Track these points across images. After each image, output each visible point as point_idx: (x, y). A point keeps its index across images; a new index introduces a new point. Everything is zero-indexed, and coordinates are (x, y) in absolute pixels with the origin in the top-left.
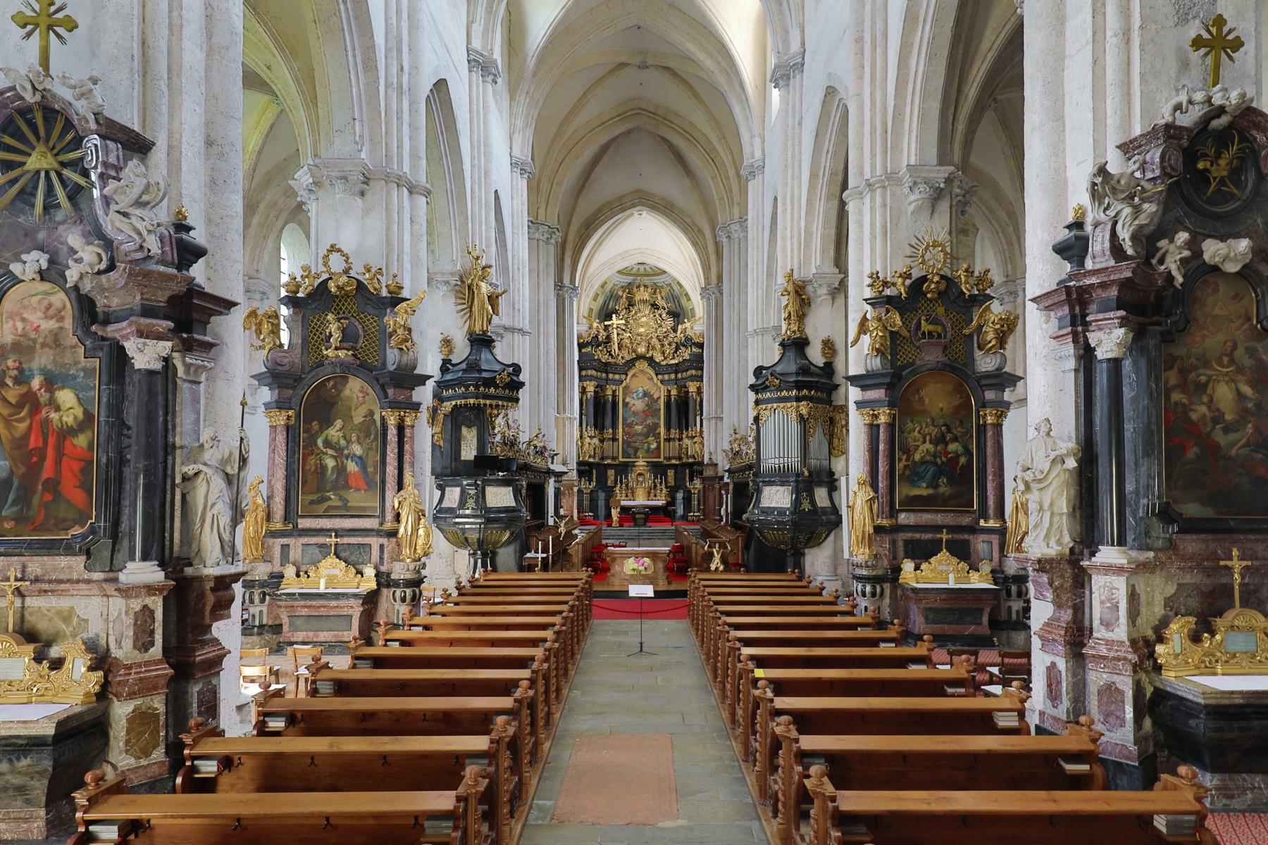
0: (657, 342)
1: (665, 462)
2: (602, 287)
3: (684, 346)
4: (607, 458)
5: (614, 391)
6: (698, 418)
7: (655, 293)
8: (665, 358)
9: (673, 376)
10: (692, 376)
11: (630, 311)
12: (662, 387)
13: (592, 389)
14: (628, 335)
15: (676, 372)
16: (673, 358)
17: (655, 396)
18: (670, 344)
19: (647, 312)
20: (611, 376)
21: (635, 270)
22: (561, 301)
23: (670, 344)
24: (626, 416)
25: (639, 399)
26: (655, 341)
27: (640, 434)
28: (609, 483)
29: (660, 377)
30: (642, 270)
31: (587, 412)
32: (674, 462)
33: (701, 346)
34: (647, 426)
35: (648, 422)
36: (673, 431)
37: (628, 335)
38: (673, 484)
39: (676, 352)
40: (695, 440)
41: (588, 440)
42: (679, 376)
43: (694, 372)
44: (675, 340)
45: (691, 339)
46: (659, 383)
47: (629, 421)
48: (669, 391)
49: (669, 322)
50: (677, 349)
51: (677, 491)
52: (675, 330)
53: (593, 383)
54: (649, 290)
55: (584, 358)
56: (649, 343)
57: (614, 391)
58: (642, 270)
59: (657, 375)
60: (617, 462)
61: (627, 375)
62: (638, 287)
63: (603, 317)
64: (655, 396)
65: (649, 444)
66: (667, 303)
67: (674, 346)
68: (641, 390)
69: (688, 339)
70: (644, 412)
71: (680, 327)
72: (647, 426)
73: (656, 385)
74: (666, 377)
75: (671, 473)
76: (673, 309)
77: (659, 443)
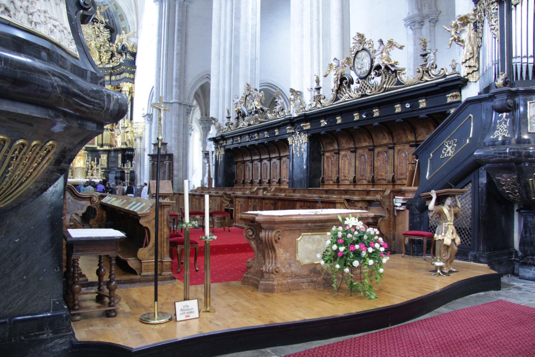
1: (99, 148)
3: (120, 53)
10: (126, 78)
15: (111, 75)
18: (106, 52)
23: (106, 52)
32: (106, 148)
33: (134, 55)
39: (111, 58)
40: (127, 130)
42: (113, 78)
43: (127, 75)
49: (106, 34)
50: (113, 55)
51: (109, 172)
52: (112, 40)
66: (105, 18)
67: (110, 53)
69: (124, 48)
71: (118, 36)
75: (104, 158)
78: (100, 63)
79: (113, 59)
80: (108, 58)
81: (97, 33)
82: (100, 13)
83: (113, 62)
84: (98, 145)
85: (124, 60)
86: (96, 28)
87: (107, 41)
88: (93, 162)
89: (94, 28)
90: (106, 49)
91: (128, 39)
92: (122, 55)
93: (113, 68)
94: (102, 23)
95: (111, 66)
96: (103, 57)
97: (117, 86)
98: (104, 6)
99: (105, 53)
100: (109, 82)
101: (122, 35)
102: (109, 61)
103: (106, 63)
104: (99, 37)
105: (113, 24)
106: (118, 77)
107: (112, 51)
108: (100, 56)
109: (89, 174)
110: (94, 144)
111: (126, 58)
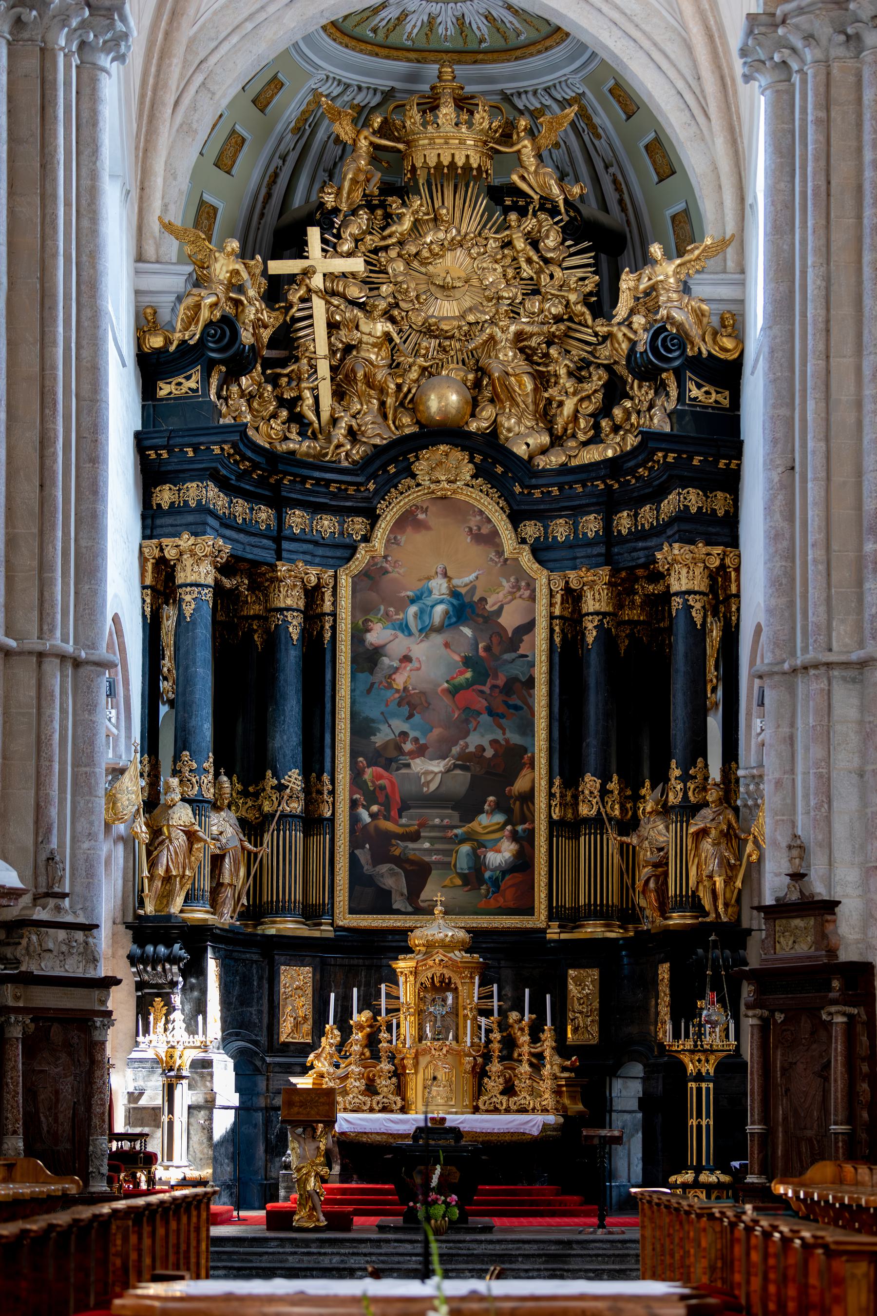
0: (520, 365)
2: (261, 102)
4: (279, 910)
5: (313, 594)
6: (714, 725)
7: (507, 136)
8: (557, 440)
9: (591, 525)
10: (683, 516)
11: (389, 219)
12: (541, 577)
13: (205, 573)
14: (381, 327)
16: (596, 439)
17: (509, 620)
18: (578, 374)
19: (470, 225)
20: (297, 520)
21: (413, 26)
22: (31, 64)
24: (371, 709)
25: (428, 630)
26: (508, 354)
27: (436, 800)
28: (286, 1032)
29: (531, 529)
30: (446, 27)
31: (184, 683)
32: (593, 930)
34: (465, 761)
35: (474, 741)
36: (590, 783)
37: (381, 327)
38: (592, 1036)
39: (605, 411)
41: (182, 815)
42: (624, 522)
43: (693, 499)
44: (604, 353)
45: (682, 339)
46: (526, 559)
47: (379, 739)
48: (573, 596)
53: (209, 542)
54: (482, 119)
55: (173, 423)
56: (481, 371)
57: (313, 594)
58: (446, 27)
59: (516, 519)
60: (326, 931)
61: (373, 518)
62: (430, 105)
63: (267, 237)
64: (509, 620)
65: (479, 845)
67: (598, 379)
68: (439, 587)
70: (454, 691)
71: (627, 282)
72: (465, 761)
73: (510, 567)
74: (561, 530)
76: (591, 210)
77: (525, 841)
78: (545, 439)
79: (617, 412)
80: (589, 408)
81: (527, 271)
82: (539, 157)
83: (616, 429)
84: (550, 918)
85: (669, 416)
86: (520, 244)
87: (579, 307)
88: (514, 1016)
89: (508, 244)
90: (578, 352)
91: (686, 289)
92: (661, 388)
93: (613, 466)
94: (554, 212)
95: (610, 453)
96: (561, 404)
97: (645, 566)
98: (564, 104)
99: (569, 384)
100: (602, 549)
101: (648, 271)
102: (597, 427)
103: (582, 437)
104: (536, 292)
105: (621, 201)
106: (647, 514)
107: (608, 368)
108: (549, 401)
109: (494, 1085)
110: (530, 911)
111: (681, 398)
